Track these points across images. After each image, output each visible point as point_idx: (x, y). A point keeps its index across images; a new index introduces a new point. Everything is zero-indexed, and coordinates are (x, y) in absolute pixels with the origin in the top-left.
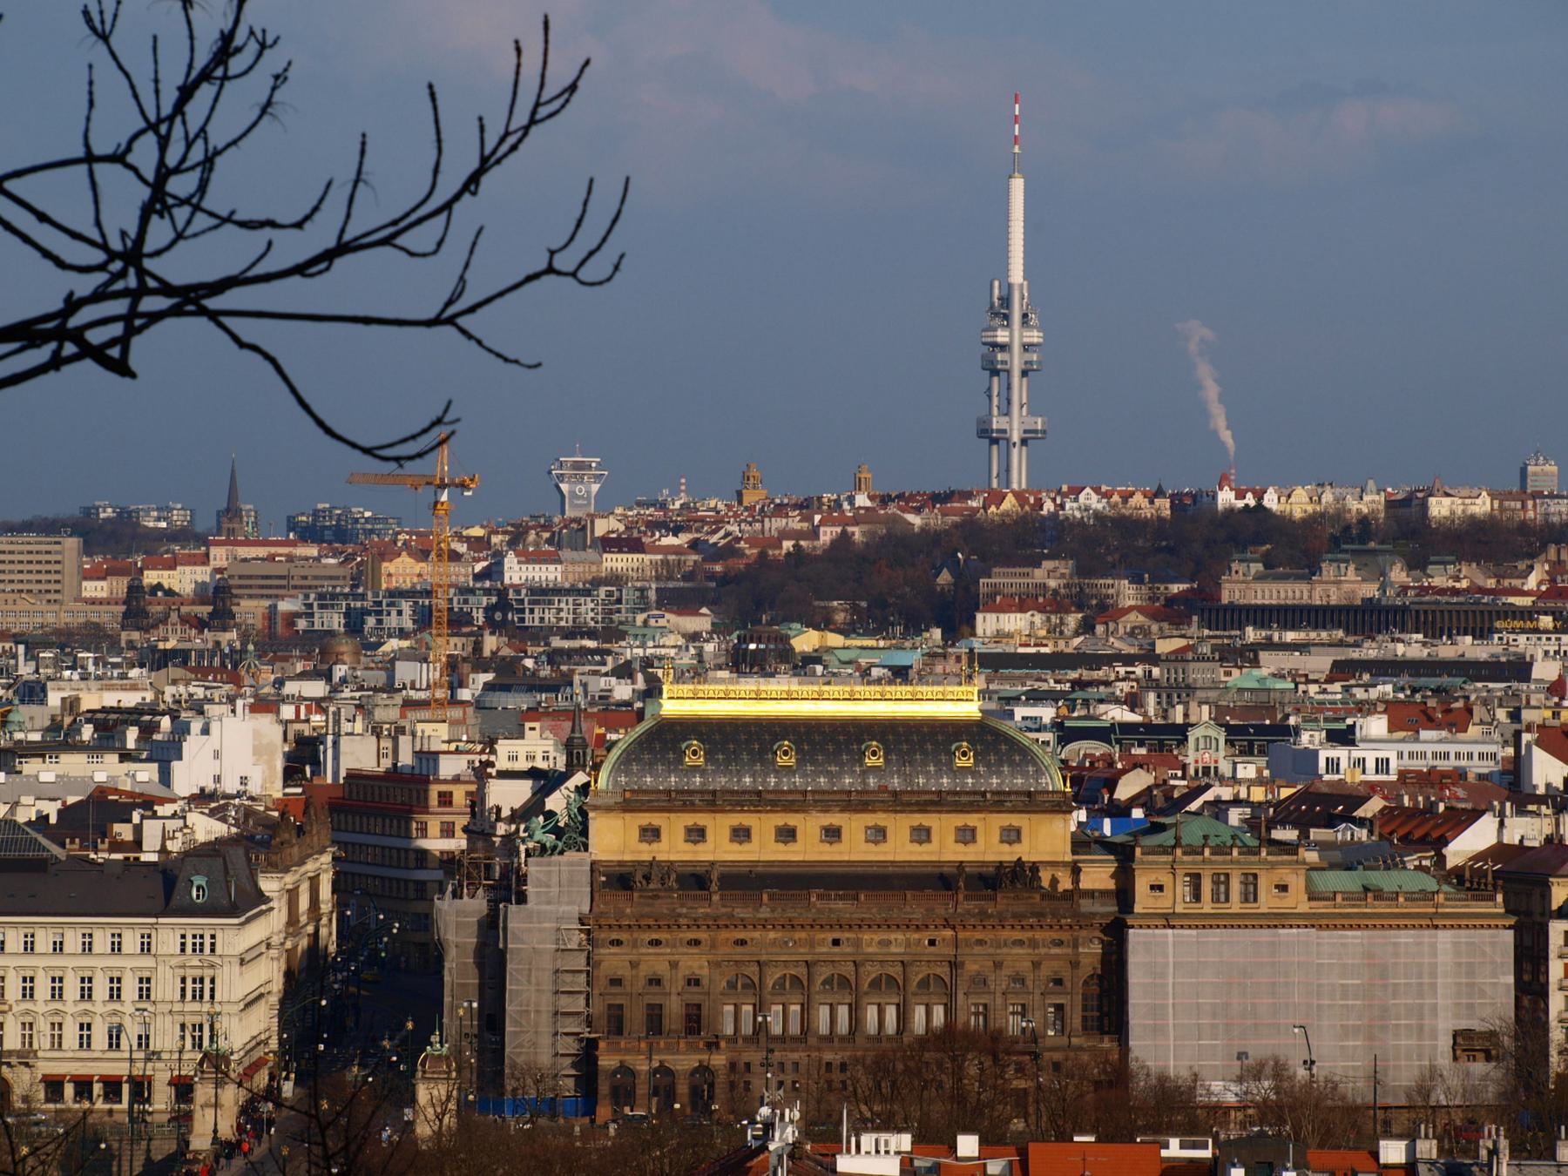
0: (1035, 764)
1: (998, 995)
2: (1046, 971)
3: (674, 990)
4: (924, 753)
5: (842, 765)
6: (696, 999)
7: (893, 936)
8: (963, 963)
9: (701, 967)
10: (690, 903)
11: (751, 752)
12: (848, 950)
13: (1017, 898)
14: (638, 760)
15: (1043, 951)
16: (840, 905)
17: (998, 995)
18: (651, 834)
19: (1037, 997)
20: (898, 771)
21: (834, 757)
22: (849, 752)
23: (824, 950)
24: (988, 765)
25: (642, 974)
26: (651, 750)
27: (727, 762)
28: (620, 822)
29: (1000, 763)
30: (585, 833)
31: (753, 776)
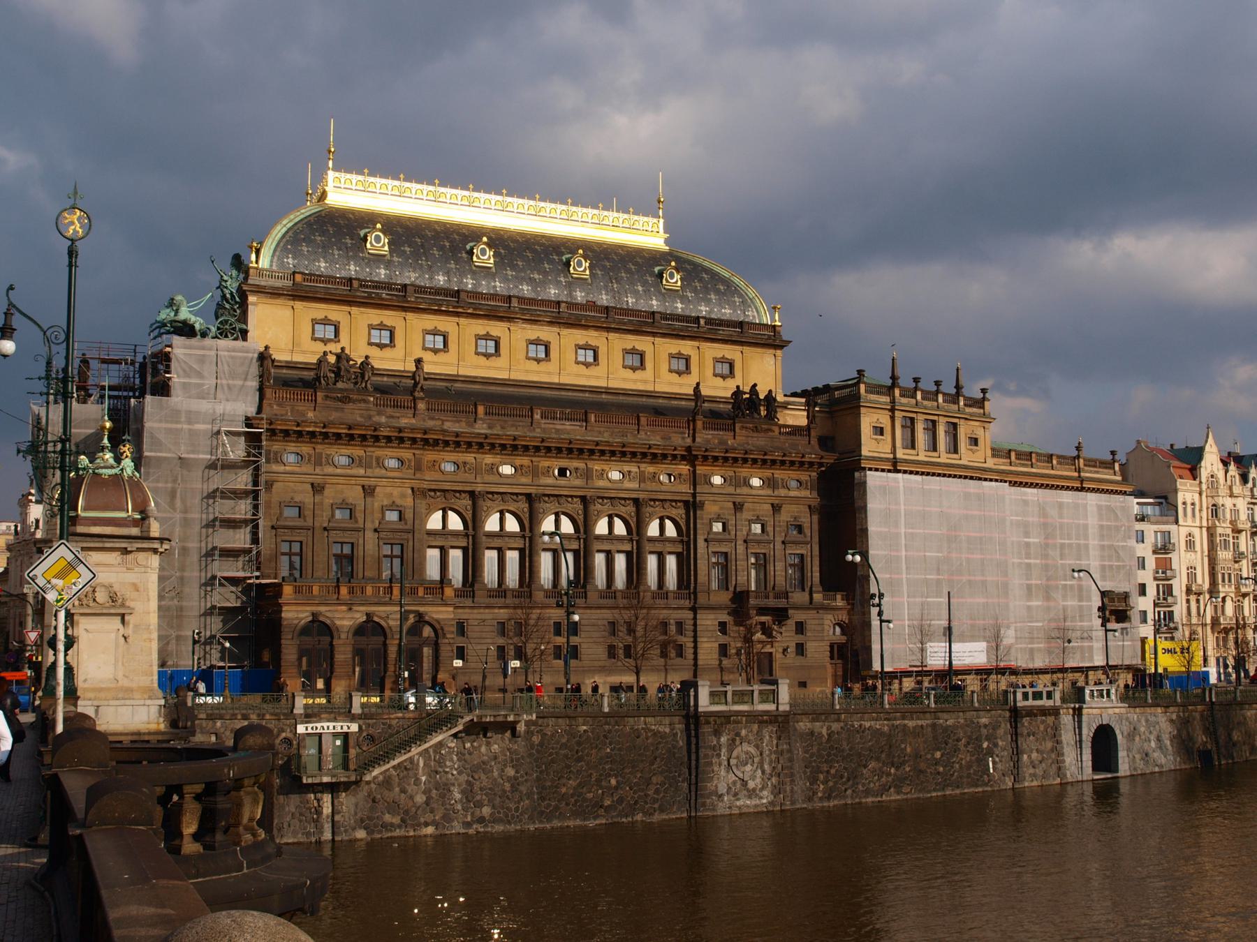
0: (741, 296)
1: (740, 542)
2: (785, 516)
3: (369, 525)
4: (628, 271)
5: (545, 273)
8: (702, 504)
9: (403, 496)
10: (389, 411)
12: (578, 482)
13: (756, 429)
14: (309, 241)
15: (783, 492)
16: (568, 425)
17: (740, 542)
19: (779, 546)
20: (606, 287)
22: (551, 262)
23: (550, 481)
24: (695, 290)
25: (328, 502)
27: (416, 255)
28: (288, 313)
29: (706, 291)
30: (244, 318)
31: (447, 273)
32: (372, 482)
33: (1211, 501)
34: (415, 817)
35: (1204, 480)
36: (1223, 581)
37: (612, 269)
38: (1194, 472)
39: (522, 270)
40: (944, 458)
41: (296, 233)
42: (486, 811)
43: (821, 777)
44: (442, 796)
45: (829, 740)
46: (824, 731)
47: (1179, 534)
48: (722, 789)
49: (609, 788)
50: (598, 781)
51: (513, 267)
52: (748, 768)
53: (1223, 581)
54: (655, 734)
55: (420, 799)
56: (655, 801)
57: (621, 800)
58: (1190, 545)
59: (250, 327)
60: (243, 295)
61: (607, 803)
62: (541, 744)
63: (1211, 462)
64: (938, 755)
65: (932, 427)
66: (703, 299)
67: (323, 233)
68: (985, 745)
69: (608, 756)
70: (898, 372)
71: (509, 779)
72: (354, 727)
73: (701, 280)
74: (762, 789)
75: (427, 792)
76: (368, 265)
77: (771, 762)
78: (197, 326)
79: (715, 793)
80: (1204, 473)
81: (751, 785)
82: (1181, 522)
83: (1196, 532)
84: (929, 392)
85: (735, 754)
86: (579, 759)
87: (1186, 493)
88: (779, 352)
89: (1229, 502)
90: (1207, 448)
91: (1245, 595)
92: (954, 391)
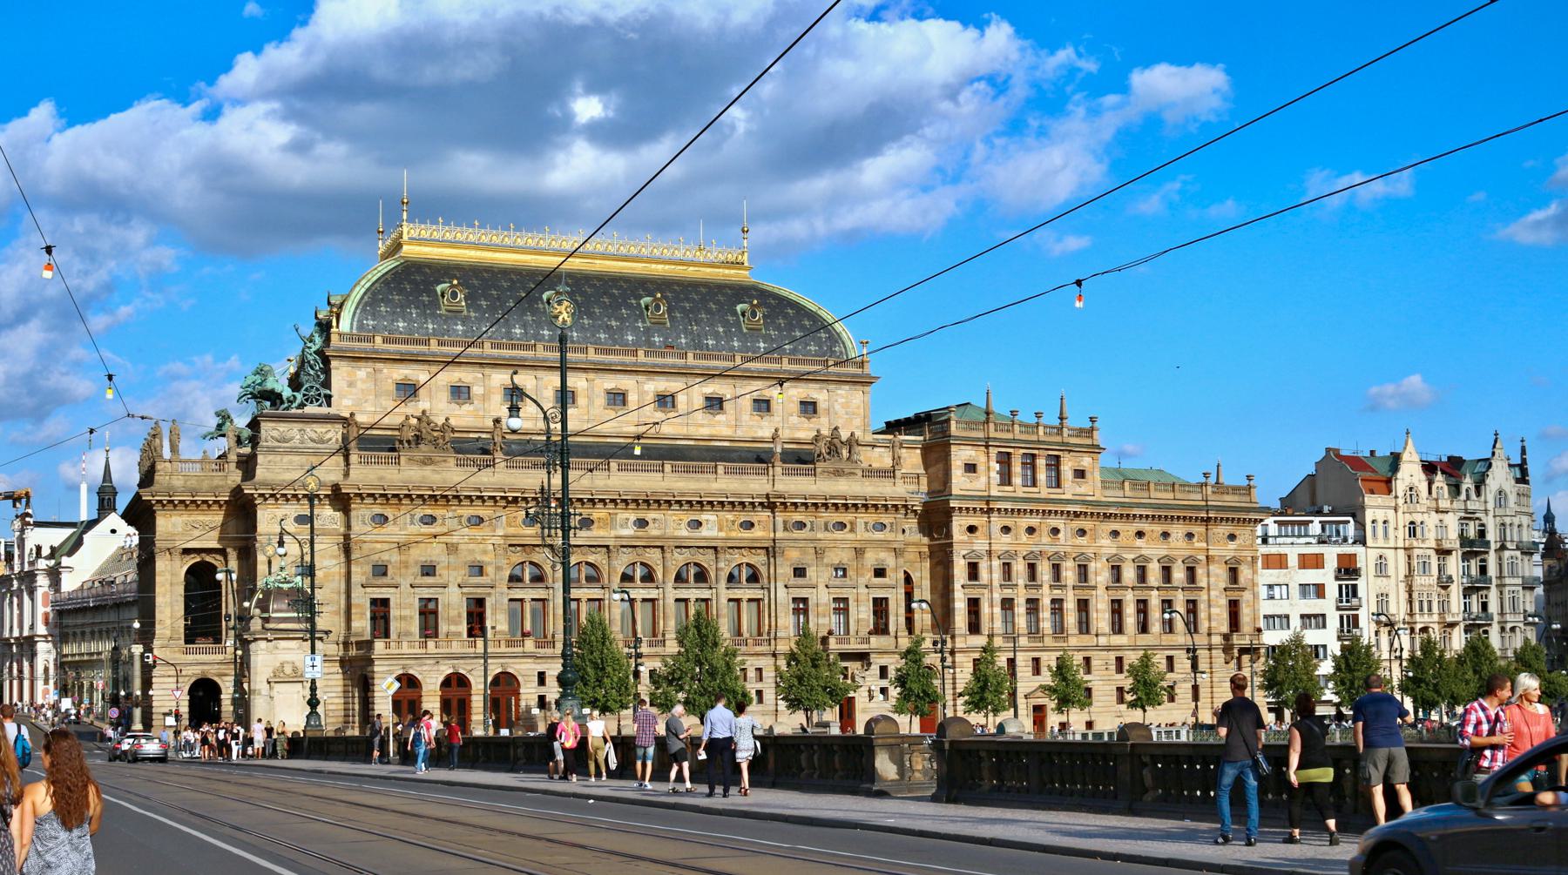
4: (709, 311)
5: (620, 319)
6: (479, 592)
7: (703, 517)
14: (387, 302)
18: (409, 390)
20: (685, 331)
21: (613, 308)
22: (629, 307)
24: (778, 328)
29: (790, 327)
30: (327, 384)
31: (524, 326)
32: (455, 539)
33: (1409, 518)
35: (1400, 494)
36: (1421, 609)
37: (691, 311)
38: (1387, 485)
40: (1043, 490)
41: (374, 294)
47: (1365, 558)
51: (591, 315)
53: (1421, 609)
58: (1381, 568)
59: (334, 391)
60: (326, 361)
63: (1410, 473)
65: (1030, 462)
67: (401, 291)
70: (994, 407)
73: (786, 316)
76: (445, 322)
80: (1400, 486)
82: (1369, 542)
83: (1389, 554)
84: (1027, 426)
87: (1376, 508)
88: (867, 389)
89: (1432, 520)
90: (1405, 457)
91: (1452, 625)
92: (1057, 422)
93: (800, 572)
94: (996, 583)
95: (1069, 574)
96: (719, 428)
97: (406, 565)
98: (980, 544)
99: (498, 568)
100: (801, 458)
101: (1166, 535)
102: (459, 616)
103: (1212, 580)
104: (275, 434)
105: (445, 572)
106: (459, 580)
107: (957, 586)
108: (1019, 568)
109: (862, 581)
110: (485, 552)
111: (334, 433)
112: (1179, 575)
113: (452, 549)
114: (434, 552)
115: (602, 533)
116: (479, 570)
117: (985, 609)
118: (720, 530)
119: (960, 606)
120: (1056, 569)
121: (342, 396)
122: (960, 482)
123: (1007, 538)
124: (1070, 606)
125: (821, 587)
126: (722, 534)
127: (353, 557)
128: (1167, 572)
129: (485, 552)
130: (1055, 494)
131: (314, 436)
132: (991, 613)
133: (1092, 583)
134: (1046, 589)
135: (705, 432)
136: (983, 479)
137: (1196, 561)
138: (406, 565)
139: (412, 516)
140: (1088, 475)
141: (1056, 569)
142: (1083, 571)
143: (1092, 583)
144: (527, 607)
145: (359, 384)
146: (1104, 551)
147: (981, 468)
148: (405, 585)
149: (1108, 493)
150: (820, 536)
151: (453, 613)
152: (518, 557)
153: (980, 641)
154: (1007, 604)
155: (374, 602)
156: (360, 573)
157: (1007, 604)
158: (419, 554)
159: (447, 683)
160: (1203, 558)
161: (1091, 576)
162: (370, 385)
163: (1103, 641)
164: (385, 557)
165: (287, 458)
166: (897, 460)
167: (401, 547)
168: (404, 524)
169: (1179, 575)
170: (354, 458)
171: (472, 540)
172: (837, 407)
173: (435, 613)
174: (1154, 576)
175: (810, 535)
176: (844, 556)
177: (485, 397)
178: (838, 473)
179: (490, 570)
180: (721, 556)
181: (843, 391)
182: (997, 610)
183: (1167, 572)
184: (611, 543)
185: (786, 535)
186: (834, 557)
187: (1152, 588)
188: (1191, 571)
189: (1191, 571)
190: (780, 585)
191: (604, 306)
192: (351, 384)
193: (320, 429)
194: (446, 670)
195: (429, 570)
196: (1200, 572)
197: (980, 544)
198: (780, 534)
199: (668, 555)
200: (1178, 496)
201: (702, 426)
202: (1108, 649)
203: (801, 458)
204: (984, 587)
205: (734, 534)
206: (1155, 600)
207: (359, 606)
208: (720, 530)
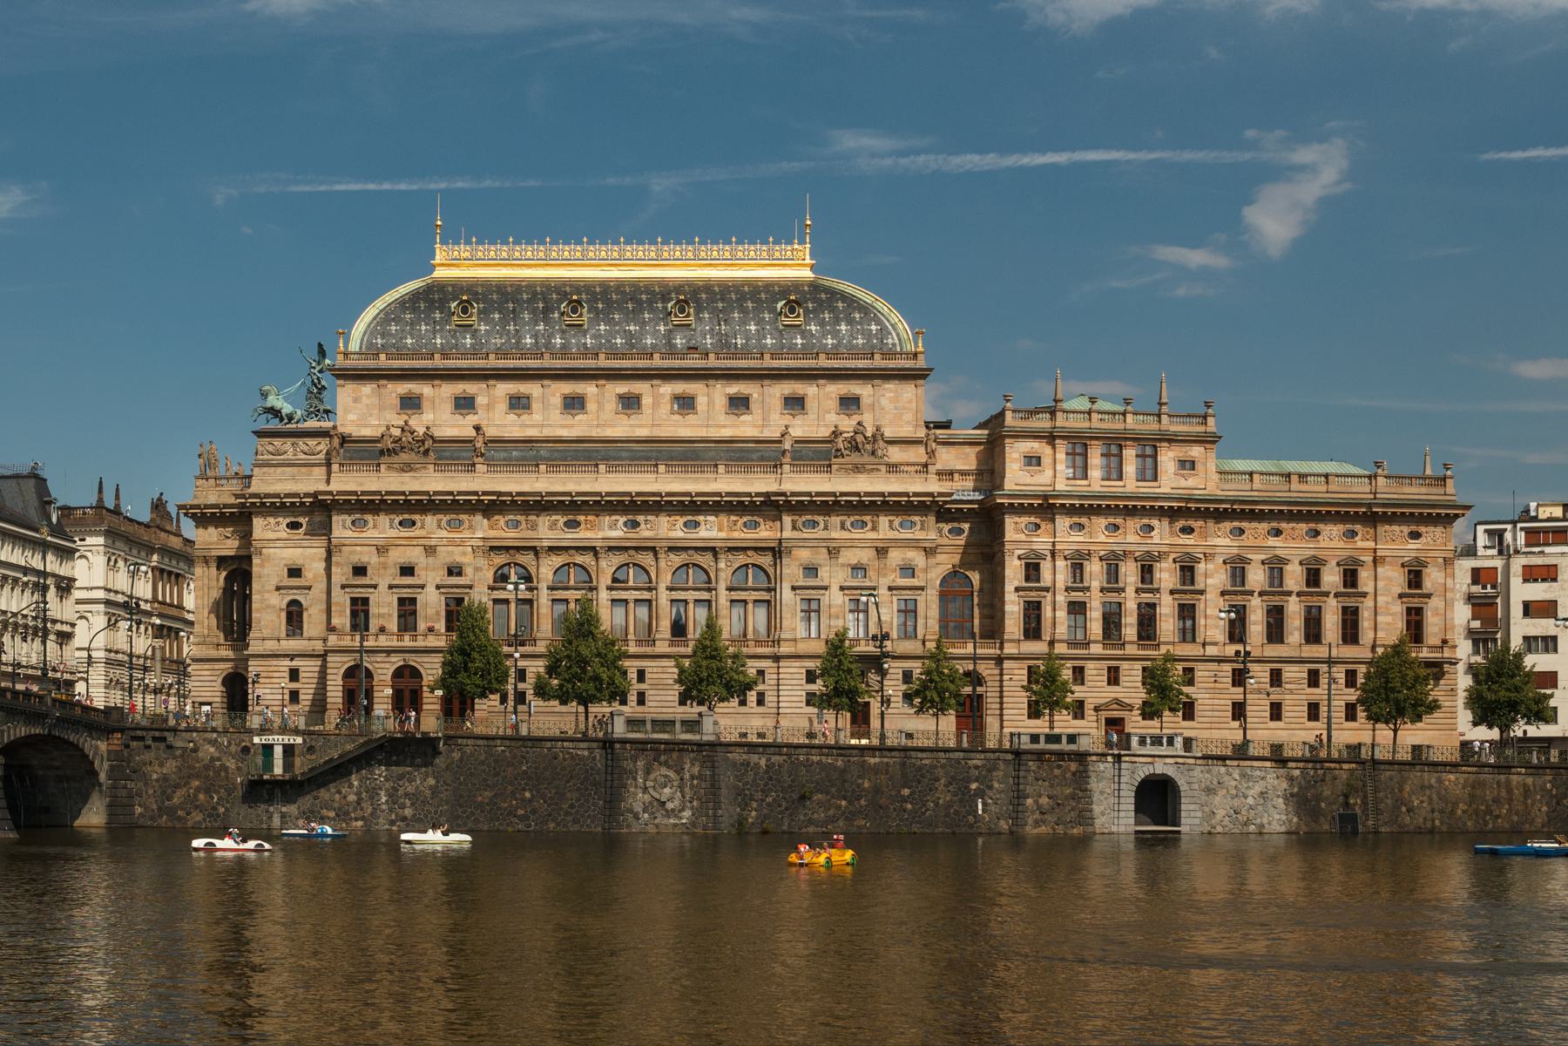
5: (643, 323)
11: (534, 312)
14: (397, 320)
18: (411, 403)
22: (652, 310)
26: (414, 310)
27: (504, 322)
34: (347, 813)
39: (617, 324)
41: (387, 314)
42: (408, 812)
43: (755, 805)
44: (372, 798)
45: (766, 772)
46: (763, 762)
48: (638, 808)
49: (524, 799)
50: (513, 793)
52: (667, 790)
54: (573, 757)
55: (352, 798)
56: (567, 813)
57: (534, 811)
61: (520, 812)
62: (461, 760)
64: (906, 792)
66: (829, 332)
68: (974, 786)
69: (525, 772)
71: (431, 787)
72: (299, 740)
73: (833, 310)
74: (683, 810)
75: (358, 794)
77: (692, 786)
78: (284, 412)
79: (631, 811)
81: (670, 806)
85: (652, 776)
86: (497, 774)
88: (920, 382)
93: (811, 570)
94: (1060, 585)
95: (1166, 576)
96: (745, 427)
97: (385, 566)
98: (1042, 542)
99: (477, 569)
100: (818, 454)
101: (1317, 533)
102: (438, 613)
103: (1380, 584)
104: (270, 448)
105: (423, 573)
106: (438, 581)
107: (1009, 588)
108: (1095, 571)
109: (884, 582)
110: (464, 554)
111: (323, 445)
112: (1331, 578)
113: (430, 550)
114: (414, 555)
115: (589, 535)
116: (454, 570)
117: (1047, 612)
118: (720, 530)
119: (1013, 607)
120: (1147, 572)
121: (346, 411)
122: (1016, 477)
123: (1078, 537)
124: (1167, 609)
125: (835, 588)
126: (723, 535)
127: (334, 559)
128: (1313, 577)
129: (464, 554)
130: (1147, 488)
131: (306, 448)
132: (1057, 619)
133: (1199, 585)
134: (1130, 591)
135: (727, 433)
136: (1049, 473)
137: (1362, 564)
138: (385, 566)
139: (392, 521)
140: (1199, 466)
141: (1147, 572)
142: (1187, 571)
143: (1199, 585)
144: (513, 606)
145: (365, 400)
146: (1218, 550)
147: (1046, 461)
148: (383, 587)
149: (1227, 487)
150: (834, 535)
151: (431, 611)
152: (500, 559)
153: (1039, 647)
154: (1077, 609)
155: (354, 601)
156: (340, 574)
157: (1077, 609)
158: (398, 556)
159: (398, 673)
160: (1368, 559)
161: (1199, 579)
162: (375, 400)
163: (1211, 651)
164: (365, 559)
165: (280, 470)
166: (931, 454)
167: (381, 550)
168: (383, 528)
169: (1331, 578)
170: (335, 467)
171: (452, 543)
172: (884, 402)
173: (414, 613)
174: (1294, 577)
175: (824, 534)
176: (865, 556)
177: (489, 407)
178: (858, 469)
179: (469, 571)
180: (722, 556)
181: (890, 386)
182: (1062, 614)
183: (1313, 577)
184: (598, 544)
185: (796, 534)
186: (850, 556)
187: (1289, 593)
188: (1350, 578)
189: (1350, 578)
190: (786, 587)
191: (626, 312)
192: (356, 400)
193: (312, 442)
194: (397, 661)
195: (407, 570)
196: (1364, 575)
197: (1042, 542)
198: (787, 534)
199: (662, 556)
200: (1332, 487)
201: (724, 426)
202: (1302, 661)
203: (818, 454)
204: (1047, 590)
205: (736, 535)
206: (1294, 610)
207: (338, 604)
208: (720, 530)
